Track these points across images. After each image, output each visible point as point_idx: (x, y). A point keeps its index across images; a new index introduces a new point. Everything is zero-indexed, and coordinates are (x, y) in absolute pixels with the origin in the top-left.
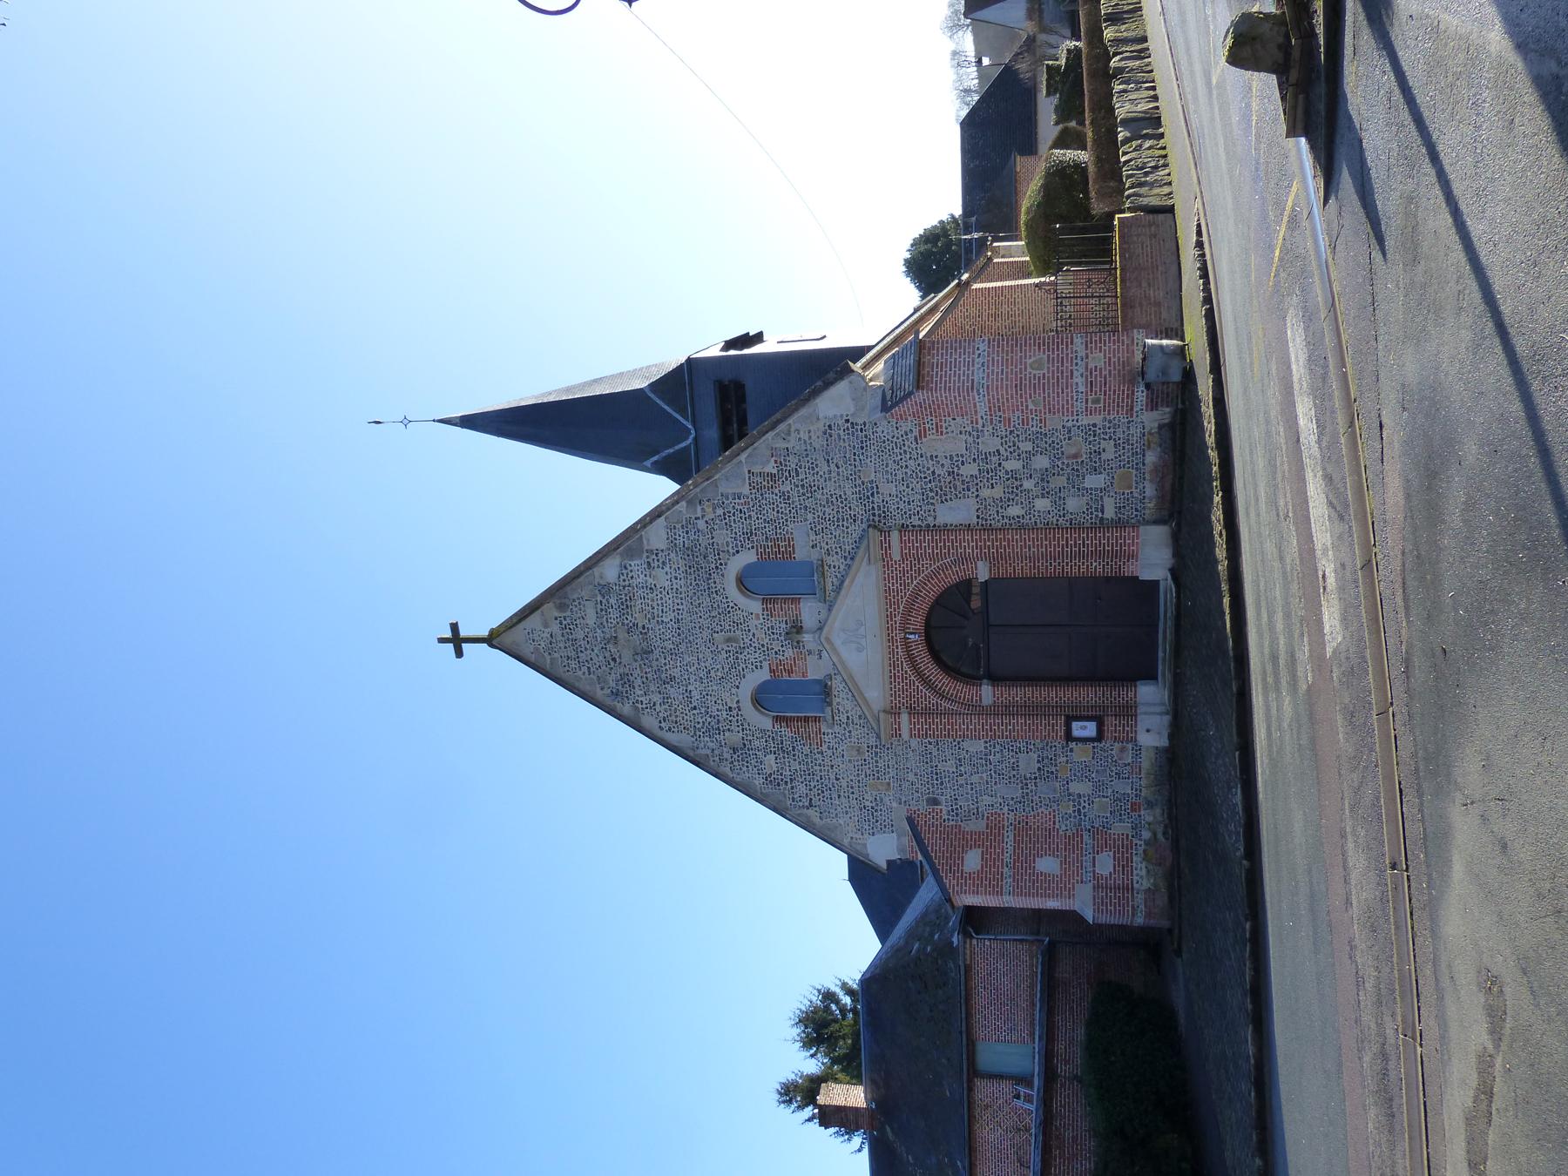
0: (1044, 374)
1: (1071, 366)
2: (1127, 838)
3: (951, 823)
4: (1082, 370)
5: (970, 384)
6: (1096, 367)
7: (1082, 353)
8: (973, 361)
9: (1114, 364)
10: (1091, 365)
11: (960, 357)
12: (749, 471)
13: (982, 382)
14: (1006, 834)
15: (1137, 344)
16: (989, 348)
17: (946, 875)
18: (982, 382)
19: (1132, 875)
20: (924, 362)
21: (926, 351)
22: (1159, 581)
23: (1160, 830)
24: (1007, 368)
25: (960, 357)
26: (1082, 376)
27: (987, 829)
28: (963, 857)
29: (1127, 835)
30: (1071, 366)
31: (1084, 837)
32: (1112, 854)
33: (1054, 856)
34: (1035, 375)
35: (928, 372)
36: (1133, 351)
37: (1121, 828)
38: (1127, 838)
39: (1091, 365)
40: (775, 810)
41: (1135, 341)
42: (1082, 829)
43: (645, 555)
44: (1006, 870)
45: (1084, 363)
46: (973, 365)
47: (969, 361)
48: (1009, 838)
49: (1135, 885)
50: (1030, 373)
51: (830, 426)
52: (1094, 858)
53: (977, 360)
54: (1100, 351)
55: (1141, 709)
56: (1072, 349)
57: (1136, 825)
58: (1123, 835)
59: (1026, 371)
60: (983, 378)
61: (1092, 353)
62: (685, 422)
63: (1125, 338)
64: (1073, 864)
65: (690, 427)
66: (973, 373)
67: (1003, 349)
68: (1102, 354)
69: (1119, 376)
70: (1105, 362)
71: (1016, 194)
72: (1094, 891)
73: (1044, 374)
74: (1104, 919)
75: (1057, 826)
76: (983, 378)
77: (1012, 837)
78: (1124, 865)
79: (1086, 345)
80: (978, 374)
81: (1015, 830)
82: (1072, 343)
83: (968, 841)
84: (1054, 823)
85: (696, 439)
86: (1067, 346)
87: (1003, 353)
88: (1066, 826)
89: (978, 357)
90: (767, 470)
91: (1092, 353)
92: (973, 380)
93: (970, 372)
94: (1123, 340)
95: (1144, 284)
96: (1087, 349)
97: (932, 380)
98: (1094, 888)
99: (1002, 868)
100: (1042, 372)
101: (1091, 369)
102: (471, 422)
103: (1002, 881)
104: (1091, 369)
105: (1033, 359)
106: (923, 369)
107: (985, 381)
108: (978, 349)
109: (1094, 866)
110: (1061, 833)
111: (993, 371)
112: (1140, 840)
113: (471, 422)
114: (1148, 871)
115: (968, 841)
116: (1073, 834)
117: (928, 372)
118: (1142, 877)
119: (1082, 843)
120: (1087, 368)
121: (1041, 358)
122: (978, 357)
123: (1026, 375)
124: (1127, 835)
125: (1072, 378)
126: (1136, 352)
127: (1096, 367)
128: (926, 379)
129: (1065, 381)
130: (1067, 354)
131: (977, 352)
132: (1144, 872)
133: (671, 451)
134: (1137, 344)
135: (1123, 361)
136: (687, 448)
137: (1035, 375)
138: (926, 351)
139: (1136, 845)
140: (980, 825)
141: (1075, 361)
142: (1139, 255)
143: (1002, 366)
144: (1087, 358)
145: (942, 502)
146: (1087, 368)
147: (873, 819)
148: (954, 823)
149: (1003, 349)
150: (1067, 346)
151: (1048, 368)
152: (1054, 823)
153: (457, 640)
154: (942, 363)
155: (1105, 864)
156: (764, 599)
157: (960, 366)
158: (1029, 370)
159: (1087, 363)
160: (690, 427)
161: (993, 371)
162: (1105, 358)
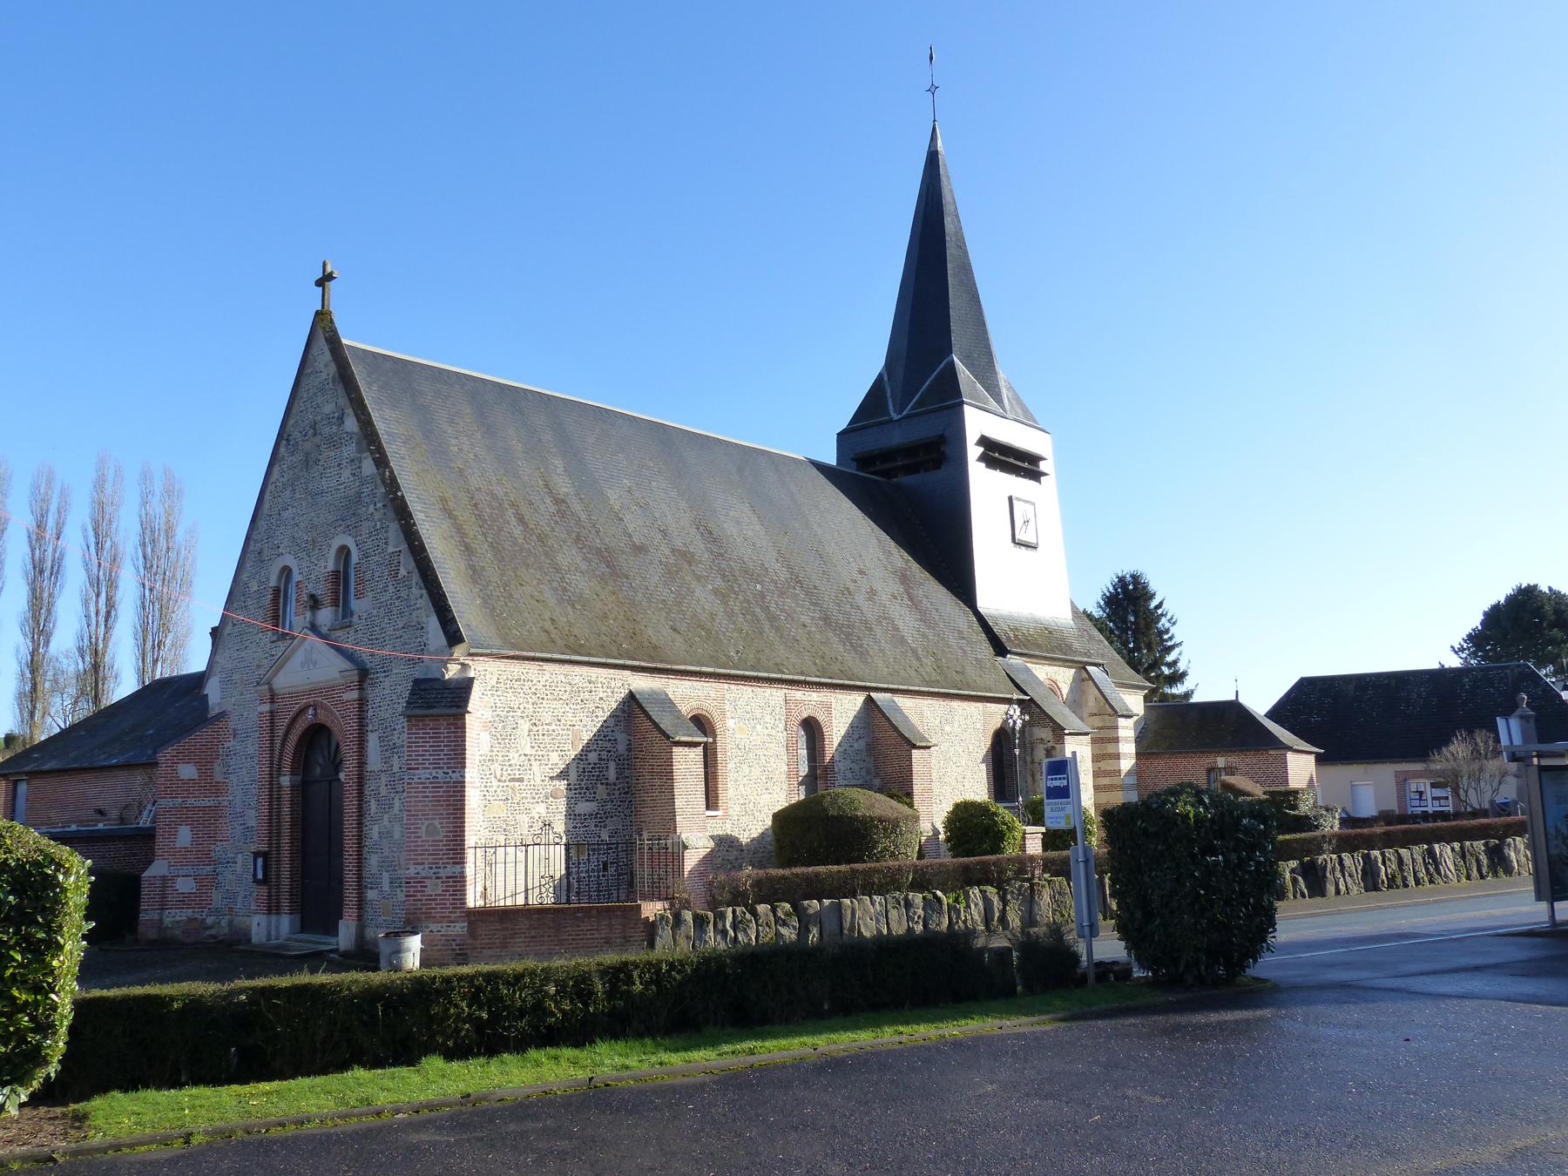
0: (420, 837)
1: (429, 863)
2: (208, 904)
3: (221, 750)
4: (423, 874)
5: (413, 766)
6: (426, 887)
7: (443, 873)
8: (439, 768)
9: (429, 904)
10: (428, 882)
11: (444, 755)
12: (400, 551)
13: (416, 778)
14: (211, 799)
15: (449, 926)
16: (454, 782)
17: (175, 749)
18: (416, 778)
19: (176, 908)
20: (439, 720)
21: (452, 721)
22: (338, 936)
23: (213, 932)
24: (430, 801)
25: (444, 755)
26: (418, 873)
27: (216, 782)
28: (190, 763)
29: (211, 904)
30: (429, 863)
31: (208, 867)
32: (194, 891)
33: (192, 841)
34: (420, 828)
35: (429, 725)
36: (441, 922)
37: (216, 898)
38: (208, 904)
39: (428, 882)
40: (231, 594)
41: (452, 925)
42: (215, 864)
43: (359, 455)
44: (180, 800)
45: (431, 875)
46: (434, 768)
47: (439, 764)
48: (208, 802)
49: (167, 911)
50: (422, 824)
51: (422, 628)
52: (190, 876)
53: (441, 771)
54: (443, 891)
55: (274, 918)
56: (448, 863)
57: (219, 912)
58: (442, 886)
59: (426, 819)
60: (420, 778)
61: (442, 882)
62: (909, 407)
63: (458, 914)
64: (185, 858)
65: (904, 413)
66: (425, 768)
67: (451, 796)
68: (440, 892)
69: (415, 909)
70: (431, 895)
71: (1241, 751)
72: (160, 877)
73: (420, 837)
74: (144, 884)
75: (218, 843)
76: (420, 778)
77: (209, 804)
78: (184, 901)
79: (451, 877)
80: (425, 773)
81: (215, 807)
82: (454, 863)
83: (205, 767)
84: (221, 841)
85: (891, 421)
86: (452, 858)
87: (447, 796)
88: (219, 851)
89: (444, 773)
90: (402, 568)
91: (442, 882)
92: (418, 768)
93: (427, 766)
94: (456, 912)
95: (533, 933)
96: (447, 877)
97: (420, 729)
98: (164, 876)
99: (181, 798)
100: (423, 835)
101: (424, 882)
102: (933, 159)
103: (171, 798)
104: (424, 882)
105: (439, 826)
106: (430, 720)
107: (416, 780)
108: (454, 772)
109: (183, 876)
110: (213, 846)
111: (428, 787)
112: (206, 915)
113: (933, 159)
114: (178, 922)
115: (205, 767)
116: (211, 858)
117: (429, 725)
118: (175, 917)
119: (203, 865)
120: (425, 878)
121: (439, 833)
122: (444, 773)
123: (421, 819)
124: (211, 904)
125: (414, 864)
126: (440, 925)
127: (426, 887)
128: (421, 724)
129: (413, 857)
130: (442, 859)
131: (450, 771)
132: (178, 918)
133: (888, 395)
134: (449, 926)
135: (431, 913)
136: (889, 414)
137: (420, 828)
138: (452, 721)
139: (202, 912)
140: (218, 777)
141: (434, 866)
142: (578, 926)
143: (432, 797)
144: (437, 878)
145: (380, 738)
146: (425, 878)
147: (227, 682)
148: (221, 753)
149: (451, 796)
150: (452, 858)
151: (427, 841)
152: (221, 841)
153: (325, 280)
154: (440, 737)
155: (185, 885)
156: (340, 572)
157: (434, 755)
158: (426, 823)
159: (431, 878)
160: (904, 413)
161: (428, 787)
162: (436, 895)
